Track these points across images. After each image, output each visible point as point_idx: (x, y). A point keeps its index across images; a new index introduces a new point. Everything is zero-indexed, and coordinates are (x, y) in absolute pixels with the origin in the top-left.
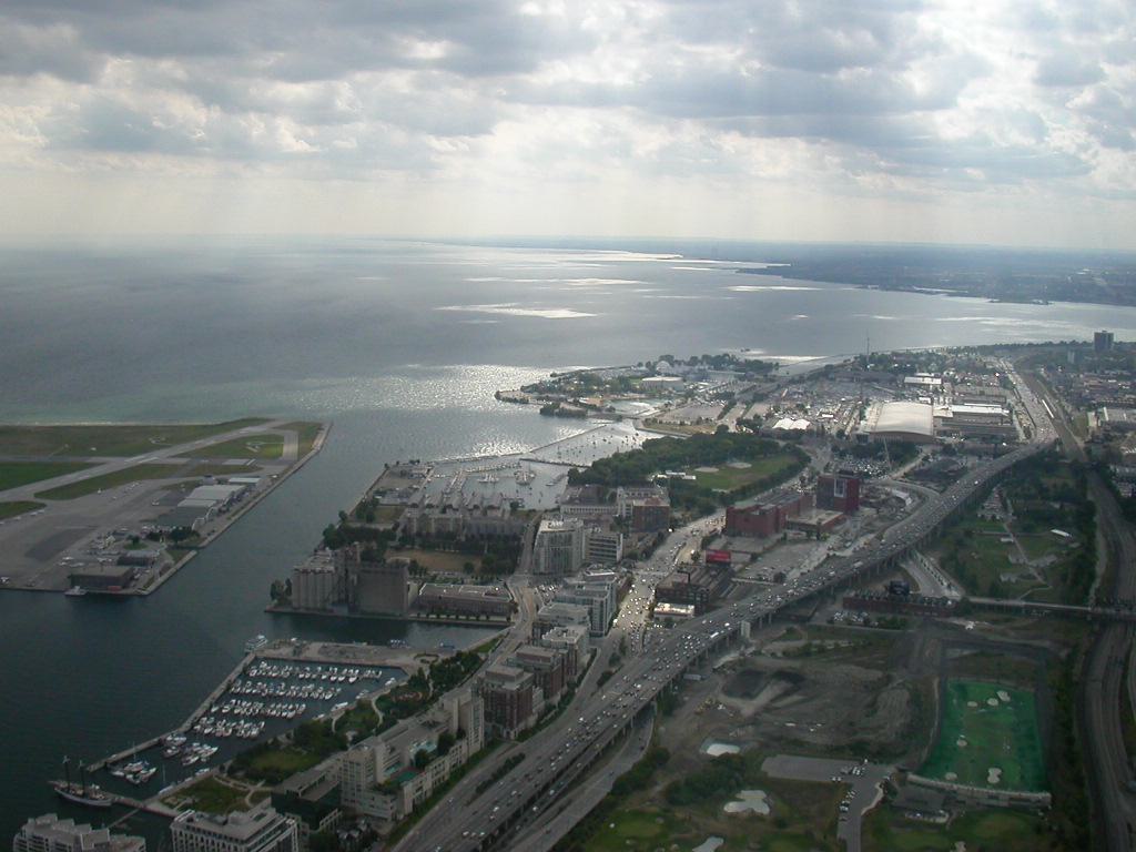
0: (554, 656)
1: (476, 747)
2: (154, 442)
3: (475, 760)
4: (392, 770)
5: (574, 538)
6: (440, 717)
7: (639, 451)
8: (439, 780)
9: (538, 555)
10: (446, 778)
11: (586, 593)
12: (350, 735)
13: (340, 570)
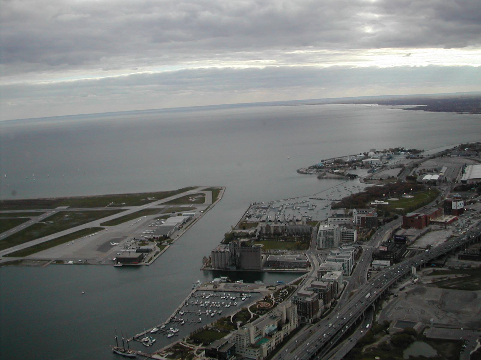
0: (328, 285)
1: (294, 327)
2: (149, 199)
3: (294, 332)
4: (258, 338)
5: (335, 233)
6: (278, 314)
7: (363, 193)
8: (278, 342)
9: (319, 241)
10: (282, 341)
11: (341, 257)
12: (239, 323)
13: (232, 250)
